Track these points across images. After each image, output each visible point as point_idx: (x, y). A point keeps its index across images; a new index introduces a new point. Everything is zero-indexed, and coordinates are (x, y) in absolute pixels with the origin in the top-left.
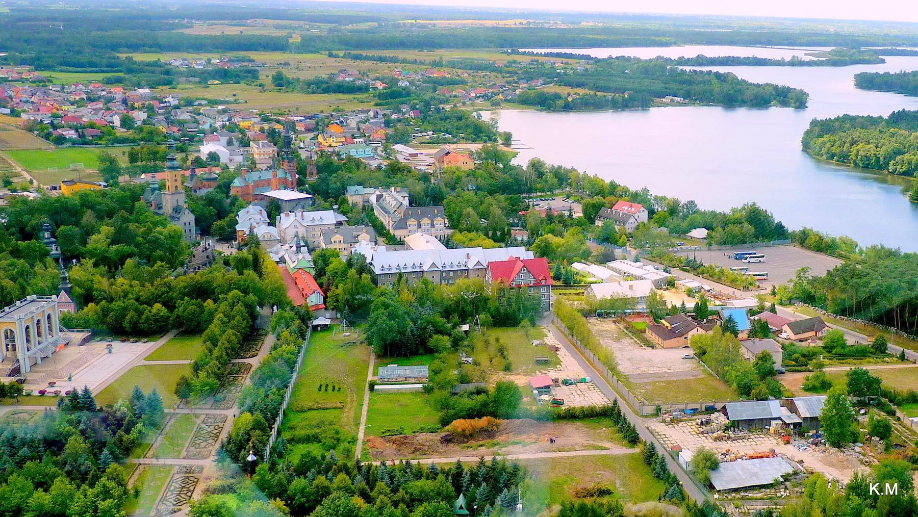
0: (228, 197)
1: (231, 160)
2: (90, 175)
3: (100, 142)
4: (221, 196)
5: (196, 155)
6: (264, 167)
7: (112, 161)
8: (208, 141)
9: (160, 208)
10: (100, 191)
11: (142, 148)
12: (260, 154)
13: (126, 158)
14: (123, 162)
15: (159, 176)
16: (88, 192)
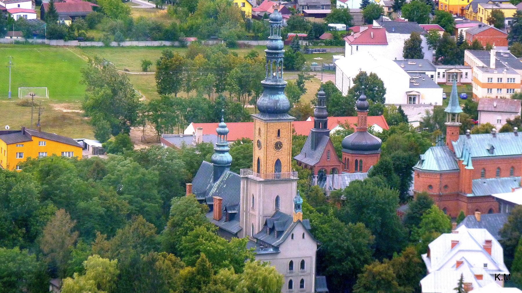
0: (404, 198)
1: (412, 99)
2: (62, 120)
3: (91, 34)
4: (386, 192)
5: (326, 78)
6: (498, 121)
7: (118, 85)
8: (357, 42)
9: (232, 217)
10: (88, 163)
11: (192, 55)
12: (489, 86)
13: (151, 79)
14: (144, 88)
15: (236, 130)
16: (61, 164)
